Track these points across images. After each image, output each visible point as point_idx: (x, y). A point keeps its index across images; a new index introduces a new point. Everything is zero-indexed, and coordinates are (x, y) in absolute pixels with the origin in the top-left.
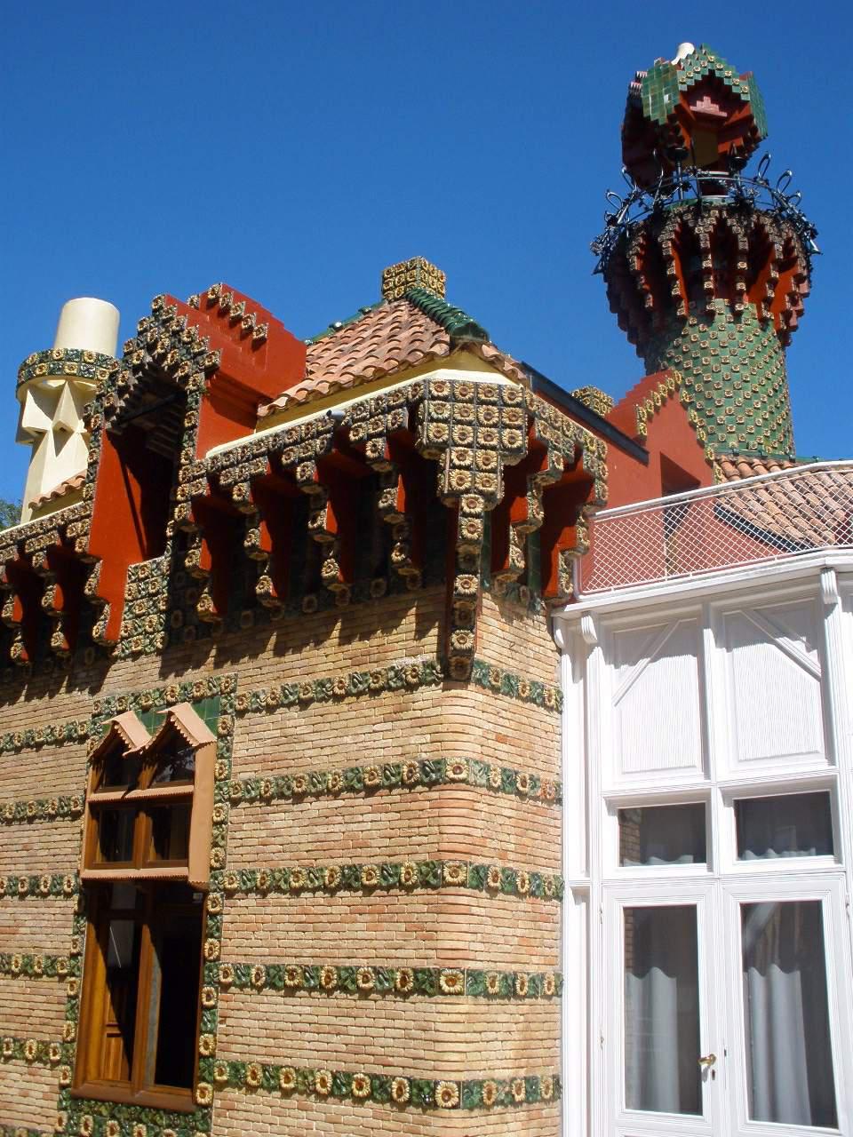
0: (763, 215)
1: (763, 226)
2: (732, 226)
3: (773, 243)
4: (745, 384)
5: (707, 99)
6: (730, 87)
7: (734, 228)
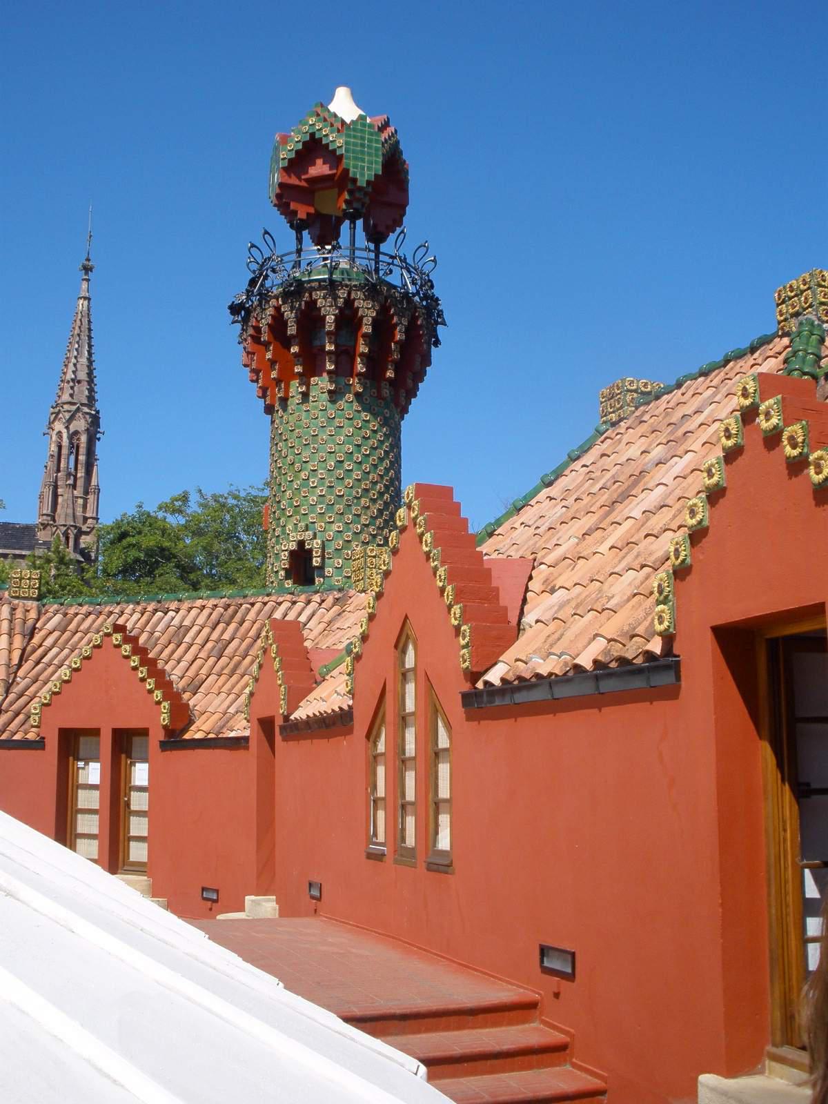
0: (316, 290)
1: (316, 301)
3: (325, 316)
4: (304, 465)
5: (319, 162)
6: (327, 145)
7: (286, 314)
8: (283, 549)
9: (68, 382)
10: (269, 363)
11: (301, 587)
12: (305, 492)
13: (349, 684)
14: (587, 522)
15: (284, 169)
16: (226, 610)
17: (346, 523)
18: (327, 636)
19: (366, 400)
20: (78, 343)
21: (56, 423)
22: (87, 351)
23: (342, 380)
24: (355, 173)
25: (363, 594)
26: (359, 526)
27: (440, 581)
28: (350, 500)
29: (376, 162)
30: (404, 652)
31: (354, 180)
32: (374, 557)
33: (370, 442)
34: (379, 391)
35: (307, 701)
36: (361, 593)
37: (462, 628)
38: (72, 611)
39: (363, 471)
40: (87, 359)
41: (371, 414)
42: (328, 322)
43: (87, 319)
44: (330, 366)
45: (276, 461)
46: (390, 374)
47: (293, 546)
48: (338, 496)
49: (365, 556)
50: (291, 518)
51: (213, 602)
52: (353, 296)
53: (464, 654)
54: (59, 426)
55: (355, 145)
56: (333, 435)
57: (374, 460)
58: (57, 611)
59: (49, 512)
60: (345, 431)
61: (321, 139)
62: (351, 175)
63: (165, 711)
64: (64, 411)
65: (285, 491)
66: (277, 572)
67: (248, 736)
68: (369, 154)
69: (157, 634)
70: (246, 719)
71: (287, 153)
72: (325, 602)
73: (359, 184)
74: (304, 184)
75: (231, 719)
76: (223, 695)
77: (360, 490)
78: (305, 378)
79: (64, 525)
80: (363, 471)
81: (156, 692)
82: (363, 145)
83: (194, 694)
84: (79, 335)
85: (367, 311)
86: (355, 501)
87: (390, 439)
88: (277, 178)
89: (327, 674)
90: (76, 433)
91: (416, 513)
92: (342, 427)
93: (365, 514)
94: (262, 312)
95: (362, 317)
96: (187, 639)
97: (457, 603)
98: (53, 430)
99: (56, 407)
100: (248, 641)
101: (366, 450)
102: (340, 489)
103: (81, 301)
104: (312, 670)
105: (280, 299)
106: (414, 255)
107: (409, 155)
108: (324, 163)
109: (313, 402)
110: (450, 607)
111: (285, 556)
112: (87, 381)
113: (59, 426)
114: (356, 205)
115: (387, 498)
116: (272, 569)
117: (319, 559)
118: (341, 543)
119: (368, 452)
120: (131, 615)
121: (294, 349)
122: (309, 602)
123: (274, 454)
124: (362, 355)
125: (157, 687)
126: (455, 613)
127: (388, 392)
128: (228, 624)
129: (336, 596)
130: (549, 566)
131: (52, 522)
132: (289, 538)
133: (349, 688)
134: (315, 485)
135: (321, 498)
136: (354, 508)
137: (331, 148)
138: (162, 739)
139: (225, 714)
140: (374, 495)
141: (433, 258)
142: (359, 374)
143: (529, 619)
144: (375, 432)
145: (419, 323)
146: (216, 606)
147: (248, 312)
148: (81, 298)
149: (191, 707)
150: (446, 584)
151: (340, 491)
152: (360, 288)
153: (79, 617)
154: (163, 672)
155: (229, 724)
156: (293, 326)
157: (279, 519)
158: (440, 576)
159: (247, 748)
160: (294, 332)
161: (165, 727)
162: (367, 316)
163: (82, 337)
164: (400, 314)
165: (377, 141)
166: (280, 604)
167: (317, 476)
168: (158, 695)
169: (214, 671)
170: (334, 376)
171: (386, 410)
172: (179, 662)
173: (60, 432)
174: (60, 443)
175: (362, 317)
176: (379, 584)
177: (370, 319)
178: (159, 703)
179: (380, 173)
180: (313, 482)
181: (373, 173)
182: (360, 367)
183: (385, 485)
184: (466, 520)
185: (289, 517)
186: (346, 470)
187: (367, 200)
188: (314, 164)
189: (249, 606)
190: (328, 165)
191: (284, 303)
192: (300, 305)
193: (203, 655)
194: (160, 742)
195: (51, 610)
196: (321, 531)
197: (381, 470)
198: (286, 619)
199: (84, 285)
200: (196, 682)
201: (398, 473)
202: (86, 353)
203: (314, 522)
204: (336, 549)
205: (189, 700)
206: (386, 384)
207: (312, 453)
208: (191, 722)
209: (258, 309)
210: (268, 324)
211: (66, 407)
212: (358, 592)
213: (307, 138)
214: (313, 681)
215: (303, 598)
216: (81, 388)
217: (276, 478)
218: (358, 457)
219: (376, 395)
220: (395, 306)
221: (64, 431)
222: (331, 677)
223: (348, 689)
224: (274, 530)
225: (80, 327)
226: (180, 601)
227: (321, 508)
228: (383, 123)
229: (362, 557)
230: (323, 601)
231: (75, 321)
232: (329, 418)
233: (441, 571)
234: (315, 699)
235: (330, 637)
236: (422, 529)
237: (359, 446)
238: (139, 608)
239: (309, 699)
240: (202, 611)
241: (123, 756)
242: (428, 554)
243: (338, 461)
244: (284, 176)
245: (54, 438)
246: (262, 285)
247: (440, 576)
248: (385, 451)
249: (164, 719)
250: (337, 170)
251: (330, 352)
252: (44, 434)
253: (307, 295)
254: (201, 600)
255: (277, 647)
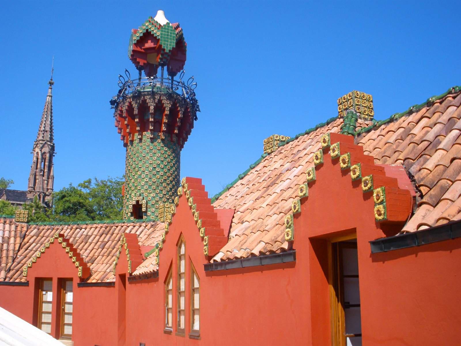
0: (146, 95)
1: (146, 100)
2: (133, 104)
4: (139, 169)
5: (150, 41)
6: (153, 35)
7: (133, 105)
8: (130, 204)
9: (42, 131)
10: (126, 126)
11: (137, 220)
12: (139, 180)
13: (157, 260)
14: (257, 194)
15: (135, 44)
16: (106, 229)
17: (157, 193)
18: (148, 240)
19: (166, 142)
20: (46, 115)
21: (36, 148)
22: (50, 118)
23: (156, 134)
24: (164, 47)
25: (163, 223)
26: (162, 195)
27: (196, 218)
28: (158, 184)
29: (173, 43)
30: (180, 247)
31: (164, 50)
32: (168, 208)
33: (167, 160)
34: (172, 138)
35: (140, 267)
36: (162, 223)
37: (205, 238)
38: (41, 228)
39: (164, 172)
40: (50, 122)
41: (168, 148)
42: (151, 109)
43: (50, 105)
44: (151, 128)
45: (128, 167)
46: (176, 131)
47: (134, 203)
48: (153, 182)
49: (164, 207)
50: (134, 191)
51: (100, 225)
52: (162, 98)
53: (205, 248)
54: (37, 150)
55: (165, 35)
56: (152, 156)
57: (169, 167)
58: (35, 228)
59: (32, 186)
60: (157, 155)
61: (150, 32)
62: (163, 47)
63: (80, 271)
64: (40, 144)
65: (131, 179)
66: (127, 213)
67: (115, 282)
68: (171, 39)
69: (77, 238)
70: (114, 274)
71: (136, 37)
72: (147, 226)
73: (166, 51)
74: (143, 51)
75: (107, 274)
76: (104, 265)
77: (162, 180)
78: (141, 132)
79: (39, 192)
80: (164, 172)
81: (76, 263)
82: (168, 35)
83: (92, 264)
84: (47, 111)
85: (167, 105)
86: (160, 184)
87: (176, 159)
88: (132, 48)
89: (148, 256)
90: (45, 153)
91: (186, 189)
92: (156, 153)
93: (164, 190)
94: (124, 104)
95: (165, 107)
96: (90, 241)
97: (203, 227)
98: (35, 151)
99: (36, 142)
100: (115, 242)
101: (165, 163)
102: (154, 179)
103: (48, 97)
104: (141, 255)
105: (131, 99)
106: (188, 80)
107: (186, 40)
108: (152, 42)
109: (144, 142)
110: (199, 229)
111: (131, 207)
112: (50, 131)
113: (37, 150)
114: (164, 60)
115: (174, 183)
116: (125, 212)
117: (145, 208)
118: (154, 202)
119: (166, 164)
120: (66, 230)
121: (136, 120)
122: (140, 226)
123: (127, 164)
124: (165, 123)
125: (77, 261)
126: (202, 231)
127: (175, 139)
128: (107, 235)
129: (152, 224)
130: (241, 212)
131: (33, 190)
132: (132, 200)
133: (157, 262)
134: (144, 177)
135: (146, 183)
136: (160, 187)
137: (155, 36)
138: (79, 282)
139: (105, 272)
140: (168, 182)
141: (195, 83)
142: (163, 131)
143: (232, 234)
144: (169, 155)
145: (189, 110)
146: (102, 227)
147: (118, 104)
148: (48, 96)
149: (91, 269)
150: (198, 219)
151: (154, 180)
152: (165, 95)
153: (45, 230)
154: (79, 254)
155: (107, 277)
156: (136, 110)
157: (129, 191)
158: (196, 216)
159: (114, 287)
160: (137, 113)
161: (80, 277)
162: (167, 107)
163: (48, 113)
164: (181, 106)
165: (174, 34)
166: (128, 227)
167: (145, 173)
168: (77, 264)
169: (101, 254)
170: (153, 132)
171: (174, 147)
172: (86, 250)
173: (37, 153)
174: (38, 157)
175: (165, 107)
176: (170, 219)
177: (169, 108)
178: (77, 267)
179: (175, 47)
180: (143, 176)
181: (172, 47)
182: (164, 128)
183: (173, 178)
184: (207, 193)
185: (133, 190)
186: (157, 171)
187: (169, 58)
188: (147, 42)
189: (116, 227)
190: (153, 43)
191: (133, 100)
192: (140, 101)
193: (96, 247)
194: (78, 284)
195: (33, 227)
196: (146, 197)
197: (171, 172)
198: (131, 233)
199: (50, 90)
200: (93, 259)
201: (179, 173)
202: (50, 119)
203: (143, 193)
204: (152, 204)
205: (90, 266)
206: (174, 136)
207: (143, 164)
208: (91, 275)
209: (122, 103)
210: (126, 109)
211: (41, 142)
212: (161, 222)
213: (145, 31)
214: (142, 259)
215: (138, 224)
216: (47, 134)
217: (128, 174)
218: (162, 166)
219: (170, 140)
220: (179, 103)
221: (40, 152)
222: (150, 257)
223: (156, 263)
224: (126, 196)
225: (47, 108)
226: (87, 224)
227: (146, 187)
228: (177, 26)
229: (163, 208)
230: (146, 226)
231: (45, 105)
232: (150, 149)
233: (196, 214)
234: (143, 266)
235: (150, 241)
236: (188, 196)
237: (162, 161)
238: (70, 227)
239: (140, 267)
240: (96, 229)
241: (62, 289)
242: (191, 207)
243: (154, 167)
244: (135, 47)
245: (35, 155)
246: (124, 93)
247: (196, 216)
248: (173, 164)
249: (79, 274)
250: (157, 45)
251: (151, 122)
252: (31, 153)
253: (142, 97)
254: (95, 224)
255: (127, 245)
